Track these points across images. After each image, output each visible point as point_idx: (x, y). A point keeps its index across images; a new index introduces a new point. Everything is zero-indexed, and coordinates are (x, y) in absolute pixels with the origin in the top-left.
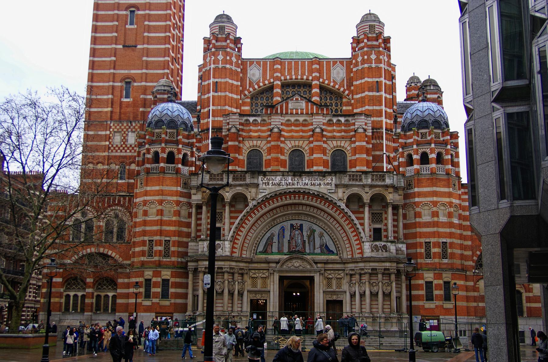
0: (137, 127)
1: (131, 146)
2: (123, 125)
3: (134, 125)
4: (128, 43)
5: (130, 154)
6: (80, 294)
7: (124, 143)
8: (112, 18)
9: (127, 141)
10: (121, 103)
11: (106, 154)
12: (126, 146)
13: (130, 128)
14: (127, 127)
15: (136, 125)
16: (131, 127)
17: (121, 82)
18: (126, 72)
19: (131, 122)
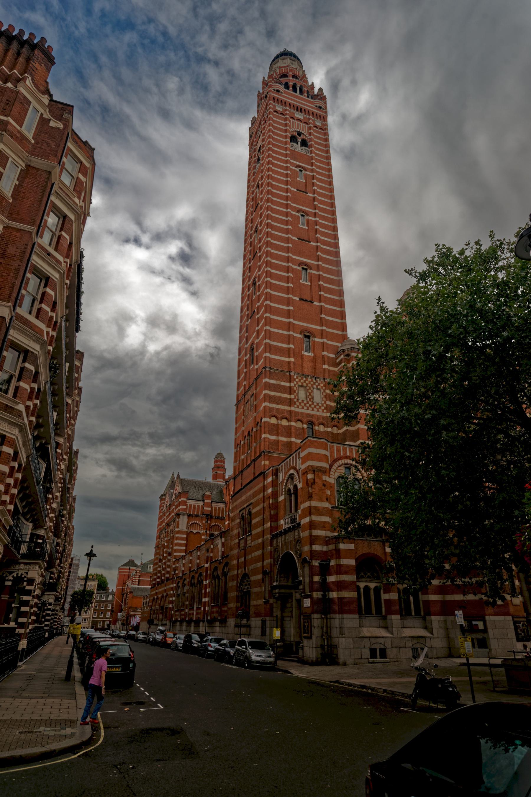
0: (322, 385)
1: (318, 404)
2: (307, 380)
3: (319, 382)
4: (303, 297)
5: (318, 413)
6: (372, 585)
7: (310, 400)
8: (287, 269)
9: (313, 397)
10: (302, 356)
11: (287, 408)
12: (313, 403)
13: (315, 384)
14: (312, 383)
15: (322, 383)
16: (316, 384)
17: (301, 333)
18: (305, 324)
19: (316, 378)
